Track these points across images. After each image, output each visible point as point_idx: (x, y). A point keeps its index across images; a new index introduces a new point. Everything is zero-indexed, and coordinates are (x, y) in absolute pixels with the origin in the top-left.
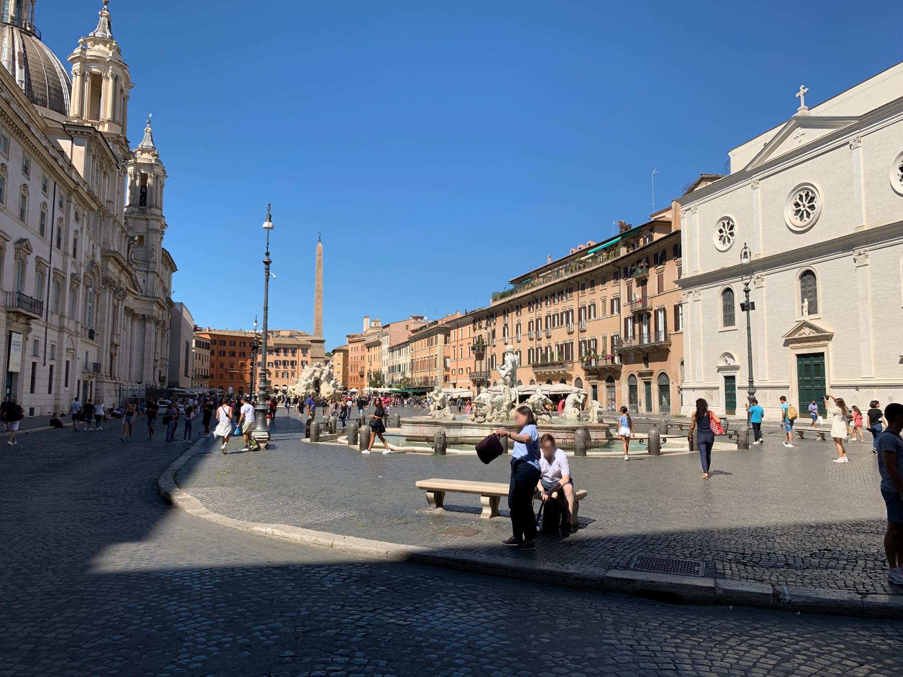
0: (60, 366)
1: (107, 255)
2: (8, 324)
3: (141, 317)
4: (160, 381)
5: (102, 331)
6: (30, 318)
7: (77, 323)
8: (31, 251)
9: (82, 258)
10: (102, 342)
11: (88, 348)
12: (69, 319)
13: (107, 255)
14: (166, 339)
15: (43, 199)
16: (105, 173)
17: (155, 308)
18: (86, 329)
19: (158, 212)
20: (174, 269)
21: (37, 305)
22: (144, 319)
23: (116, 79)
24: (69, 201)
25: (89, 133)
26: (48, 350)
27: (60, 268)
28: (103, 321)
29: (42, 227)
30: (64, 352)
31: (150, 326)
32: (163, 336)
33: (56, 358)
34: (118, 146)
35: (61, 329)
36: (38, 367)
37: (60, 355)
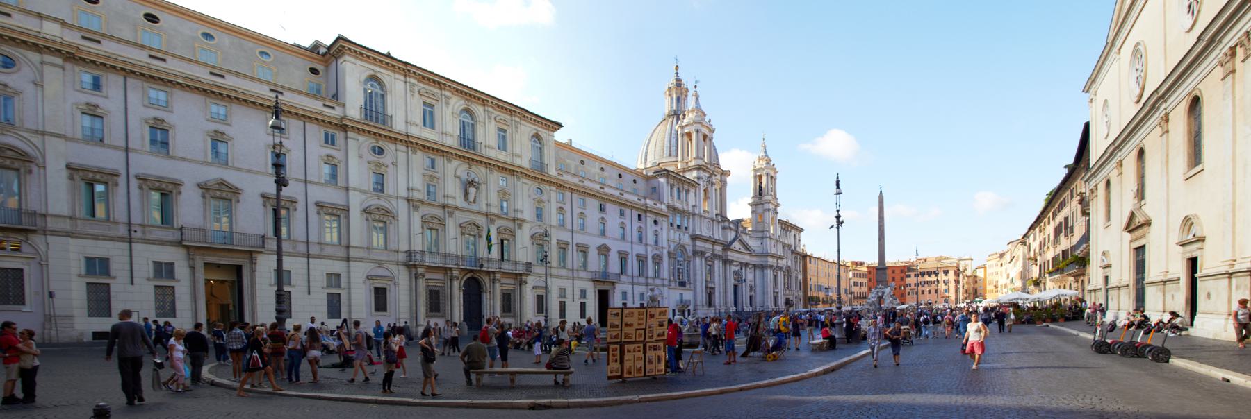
1: (694, 238)
5: (695, 281)
13: (694, 238)
17: (770, 259)
19: (769, 198)
20: (800, 230)
21: (619, 275)
22: (763, 267)
28: (695, 275)
31: (769, 272)
35: (647, 284)
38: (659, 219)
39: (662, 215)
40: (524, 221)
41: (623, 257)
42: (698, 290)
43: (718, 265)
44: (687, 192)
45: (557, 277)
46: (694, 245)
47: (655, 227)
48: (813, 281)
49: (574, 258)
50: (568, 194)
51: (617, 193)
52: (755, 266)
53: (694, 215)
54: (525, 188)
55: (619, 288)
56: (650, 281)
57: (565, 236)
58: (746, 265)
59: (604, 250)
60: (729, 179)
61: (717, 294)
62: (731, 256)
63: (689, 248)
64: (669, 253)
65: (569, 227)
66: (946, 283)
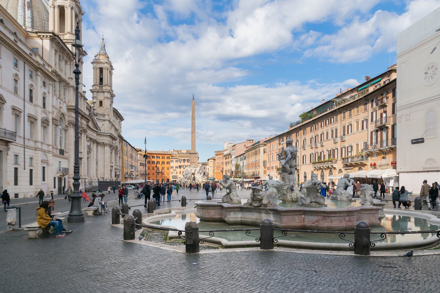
3: (102, 144)
4: (116, 177)
7: (48, 145)
8: (5, 102)
9: (49, 107)
12: (42, 143)
14: (119, 155)
15: (15, 71)
16: (66, 62)
19: (109, 88)
20: (122, 119)
21: (14, 134)
22: (104, 145)
24: (37, 75)
26: (28, 161)
27: (33, 113)
29: (16, 89)
30: (40, 162)
32: (116, 154)
33: (34, 165)
35: (36, 149)
36: (19, 170)
52: (98, 143)
55: (14, 149)
56: (39, 145)
63: (66, 117)
64: (53, 119)
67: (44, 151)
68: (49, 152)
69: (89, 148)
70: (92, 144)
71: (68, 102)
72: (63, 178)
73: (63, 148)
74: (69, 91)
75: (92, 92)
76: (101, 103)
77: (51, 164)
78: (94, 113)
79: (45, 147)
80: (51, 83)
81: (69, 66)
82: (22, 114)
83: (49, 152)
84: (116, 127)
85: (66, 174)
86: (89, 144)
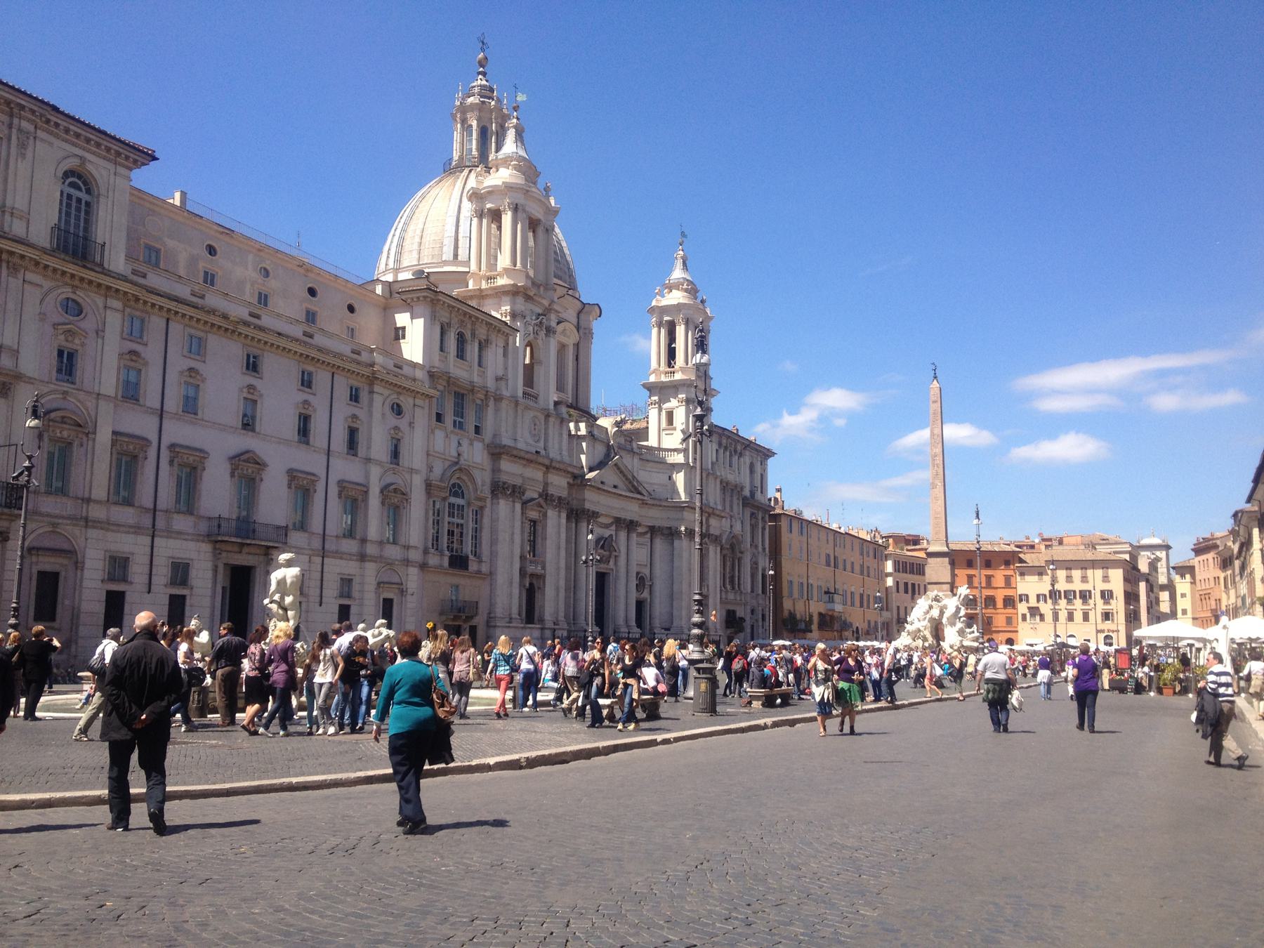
0: (361, 605)
1: (497, 452)
2: (214, 556)
3: (666, 532)
5: (493, 555)
6: (268, 548)
7: (407, 547)
10: (491, 574)
11: (455, 580)
13: (497, 452)
18: (442, 554)
20: (767, 454)
23: (516, 209)
24: (371, 392)
25: (425, 297)
28: (494, 542)
33: (355, 594)
34: (520, 300)
35: (362, 557)
37: (362, 591)
38: (406, 402)
39: (415, 394)
40: (19, 377)
41: (302, 486)
42: (501, 579)
43: (555, 522)
44: (482, 346)
45: (106, 525)
46: (496, 470)
47: (392, 420)
48: (792, 570)
49: (154, 480)
50: (156, 323)
51: (297, 331)
52: (653, 530)
53: (498, 399)
54: (33, 295)
56: (371, 550)
57: (140, 424)
58: (631, 526)
59: (247, 470)
60: (597, 326)
61: (549, 591)
62: (592, 500)
64: (429, 486)
65: (152, 400)
66: (1107, 596)
67: (390, 564)
68: (407, 562)
69: (604, 544)
70: (623, 535)
71: (495, 436)
72: (466, 626)
73: (468, 548)
74: (497, 410)
75: (649, 389)
76: (670, 415)
77: (410, 591)
78: (632, 451)
79: (393, 552)
80: (418, 402)
81: (501, 351)
82: (320, 487)
83: (407, 562)
84: (731, 478)
85: (469, 618)
86: (607, 533)
